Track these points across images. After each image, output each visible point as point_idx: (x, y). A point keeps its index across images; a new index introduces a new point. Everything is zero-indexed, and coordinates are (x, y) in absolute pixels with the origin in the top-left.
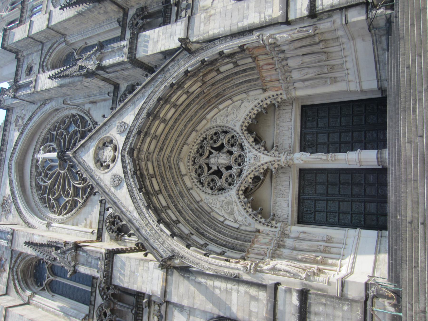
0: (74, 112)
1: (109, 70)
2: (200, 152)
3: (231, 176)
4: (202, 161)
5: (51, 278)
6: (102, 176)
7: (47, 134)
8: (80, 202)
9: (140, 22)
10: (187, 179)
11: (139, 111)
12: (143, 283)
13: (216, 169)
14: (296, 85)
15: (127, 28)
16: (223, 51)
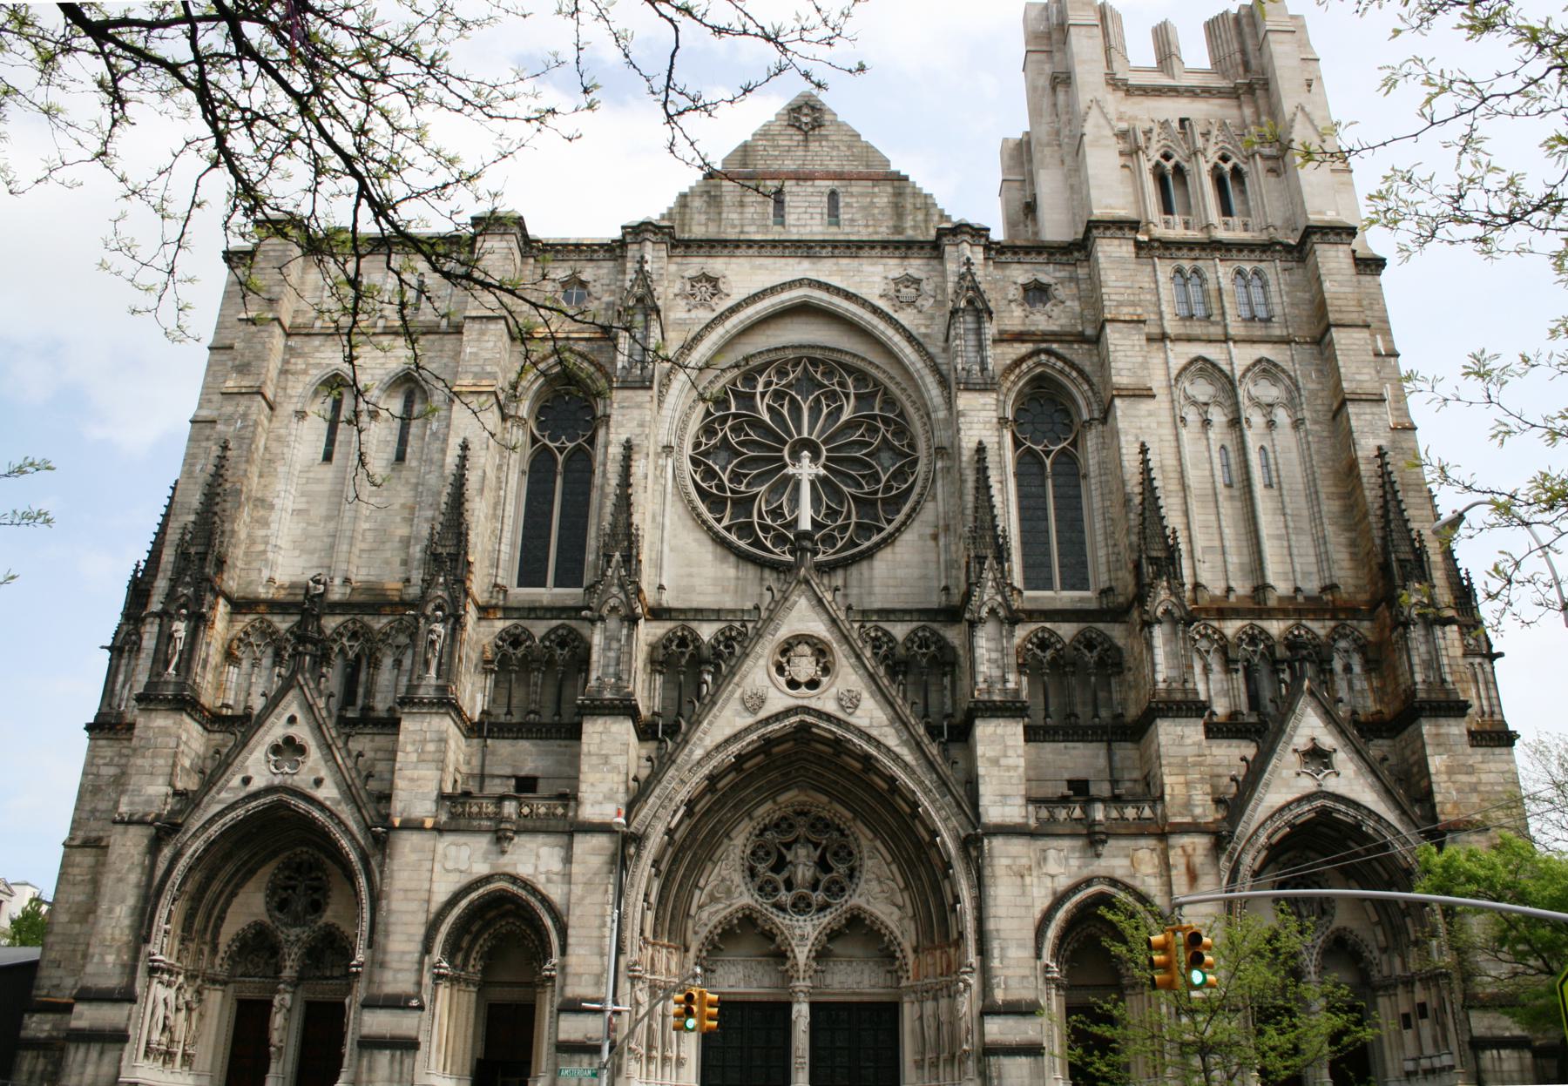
0: (921, 468)
2: (821, 825)
3: (776, 889)
4: (802, 831)
5: (560, 458)
6: (762, 662)
7: (877, 383)
8: (719, 521)
9: (1091, 657)
10: (768, 805)
13: (789, 858)
14: (916, 1005)
15: (1082, 625)
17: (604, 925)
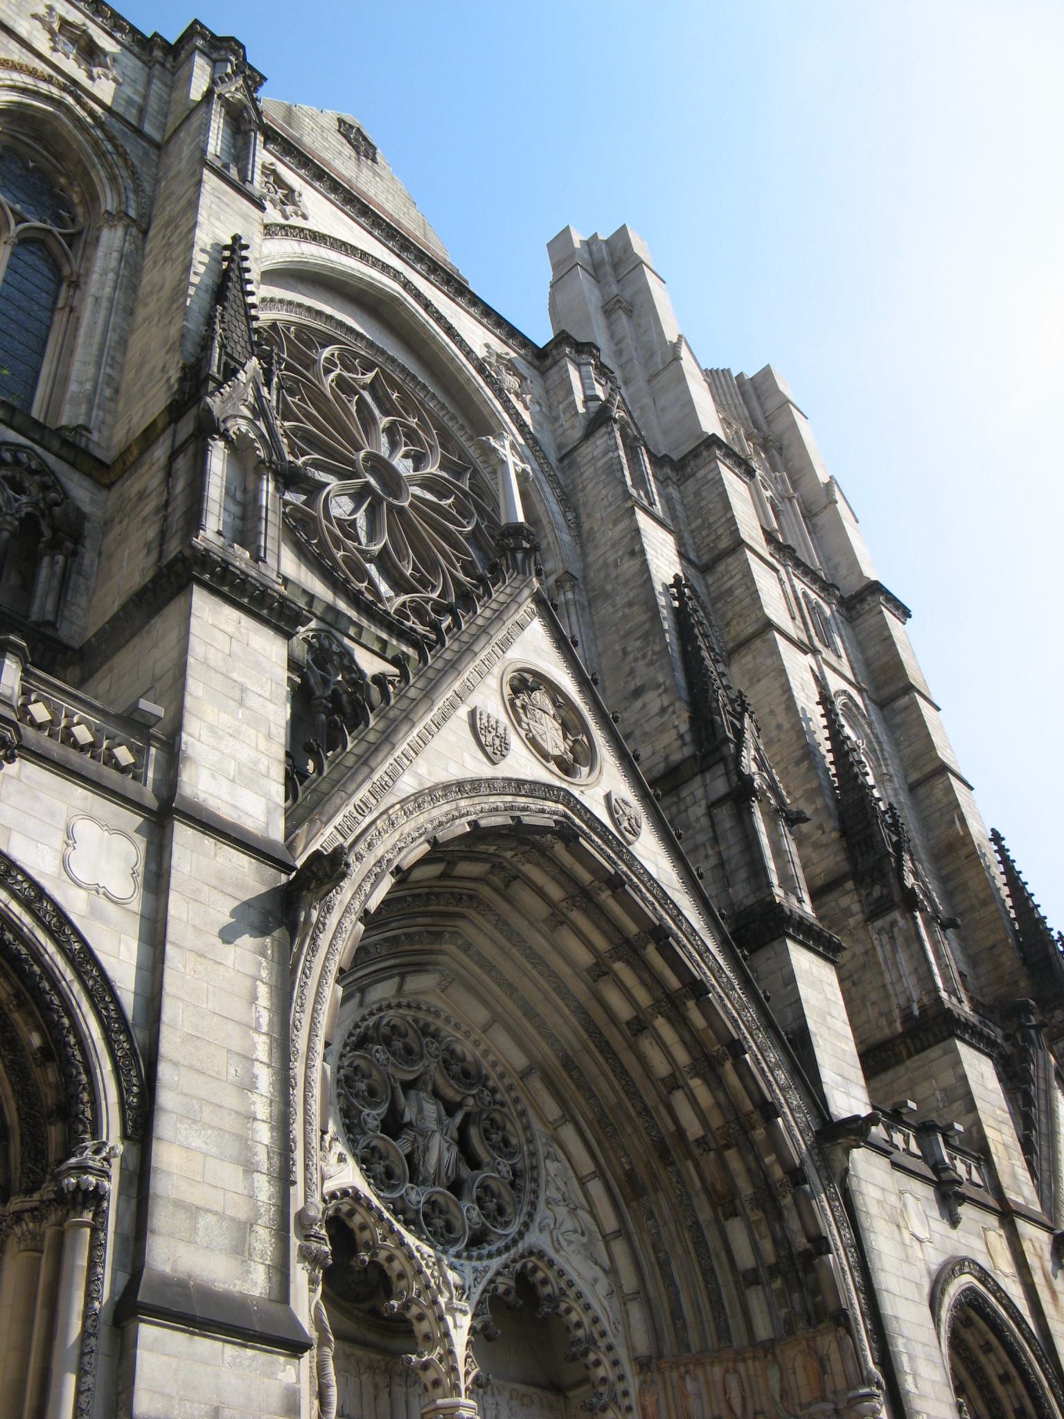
1: (724, 816)
4: (430, 1066)
6: (492, 682)
11: (672, 902)
12: (212, 730)
13: (407, 1118)
16: (829, 1251)
17: (249, 1085)
